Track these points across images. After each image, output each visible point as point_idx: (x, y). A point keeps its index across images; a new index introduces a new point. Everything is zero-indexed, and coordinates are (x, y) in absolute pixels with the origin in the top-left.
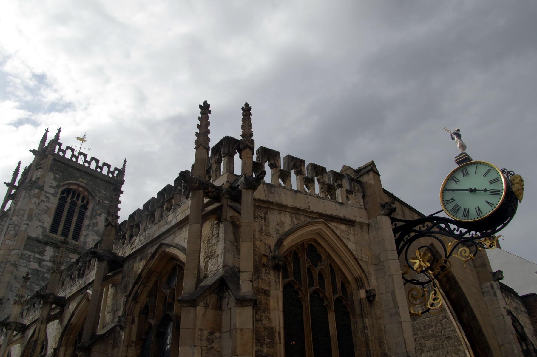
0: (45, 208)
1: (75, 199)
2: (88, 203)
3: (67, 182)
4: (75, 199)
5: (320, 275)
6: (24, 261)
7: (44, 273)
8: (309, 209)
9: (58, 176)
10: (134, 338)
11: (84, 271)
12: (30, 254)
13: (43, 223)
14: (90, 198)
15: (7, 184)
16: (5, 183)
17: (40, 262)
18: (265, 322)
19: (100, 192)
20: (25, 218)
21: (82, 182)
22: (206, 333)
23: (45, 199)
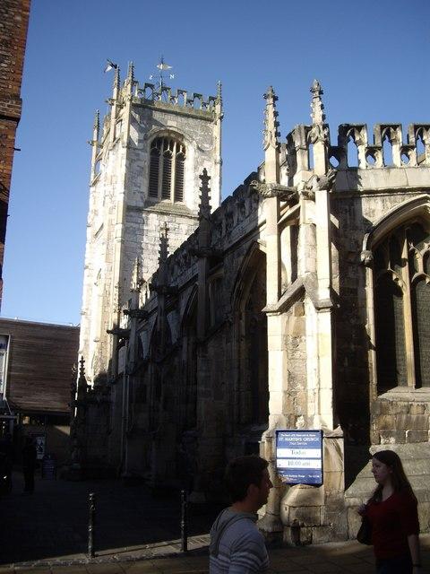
0: (138, 169)
2: (184, 151)
8: (408, 185)
9: (143, 126)
10: (243, 332)
11: (190, 260)
13: (139, 187)
18: (353, 321)
19: (196, 133)
22: (291, 338)
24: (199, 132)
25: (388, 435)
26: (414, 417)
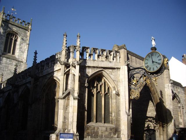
2: (17, 38)
5: (101, 86)
9: (5, 28)
10: (44, 102)
25: (88, 135)
26: (95, 131)
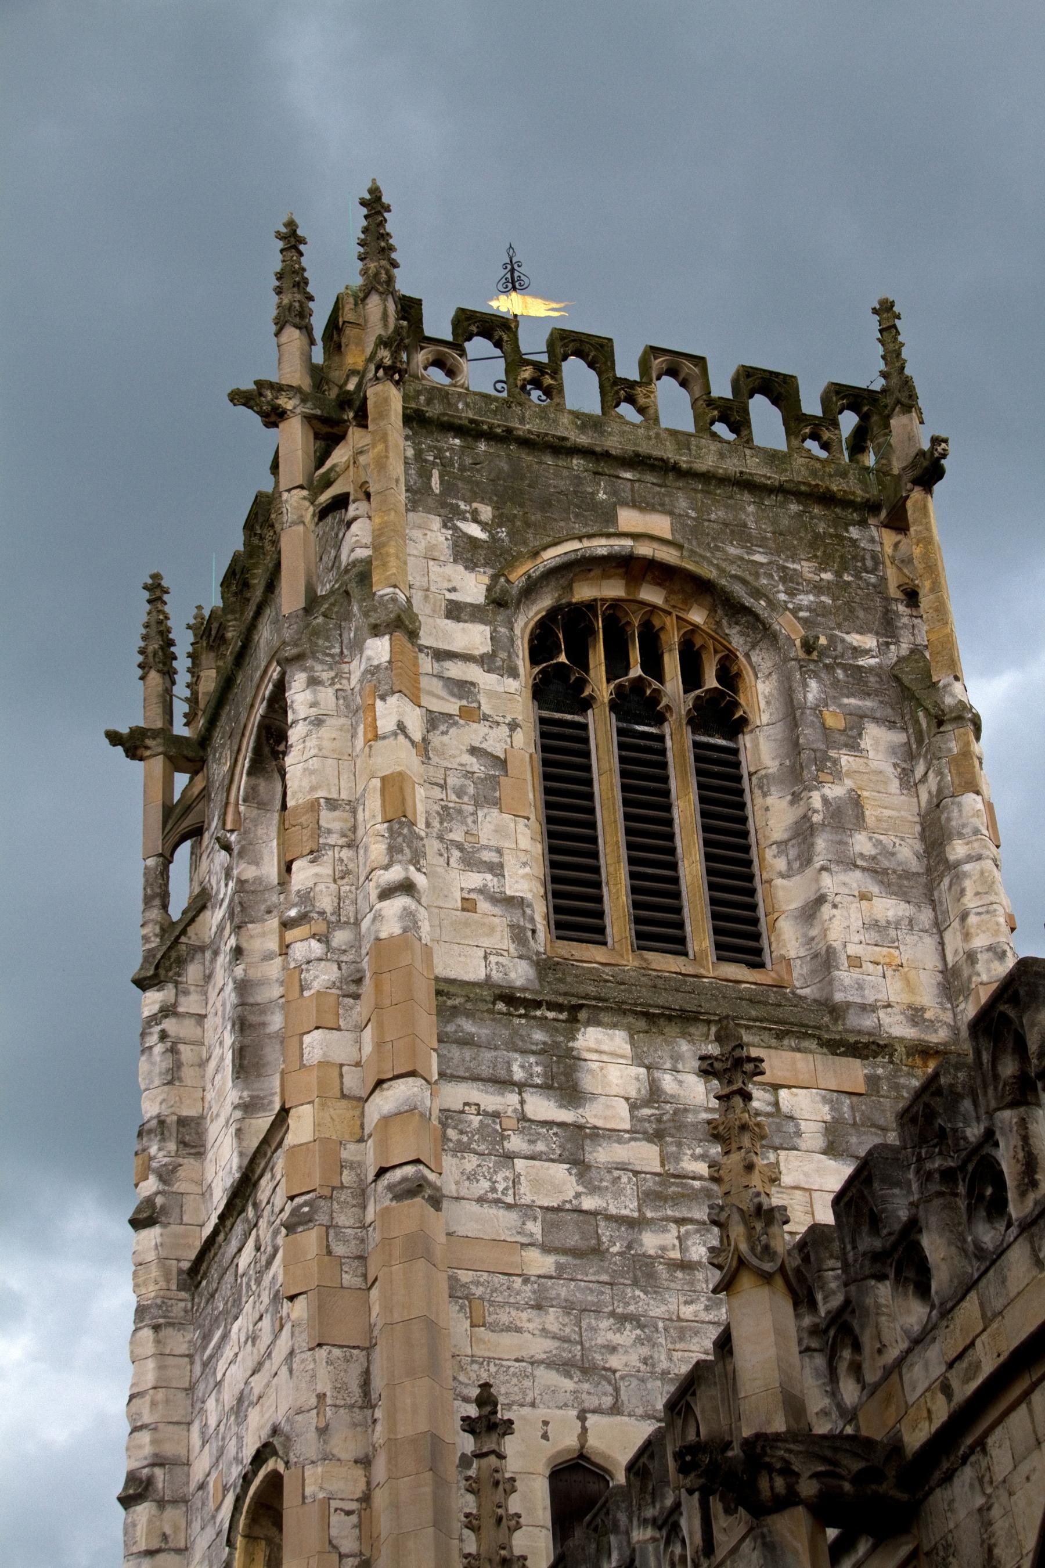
0: (474, 764)
1: (636, 671)
2: (730, 677)
3: (552, 556)
4: (636, 671)
6: (471, 1162)
7: (635, 1224)
9: (474, 530)
12: (491, 1100)
13: (497, 869)
14: (737, 641)
15: (132, 744)
16: (114, 738)
17: (575, 1144)
19: (789, 578)
20: (378, 850)
21: (645, 526)
23: (452, 706)
24: (805, 568)
